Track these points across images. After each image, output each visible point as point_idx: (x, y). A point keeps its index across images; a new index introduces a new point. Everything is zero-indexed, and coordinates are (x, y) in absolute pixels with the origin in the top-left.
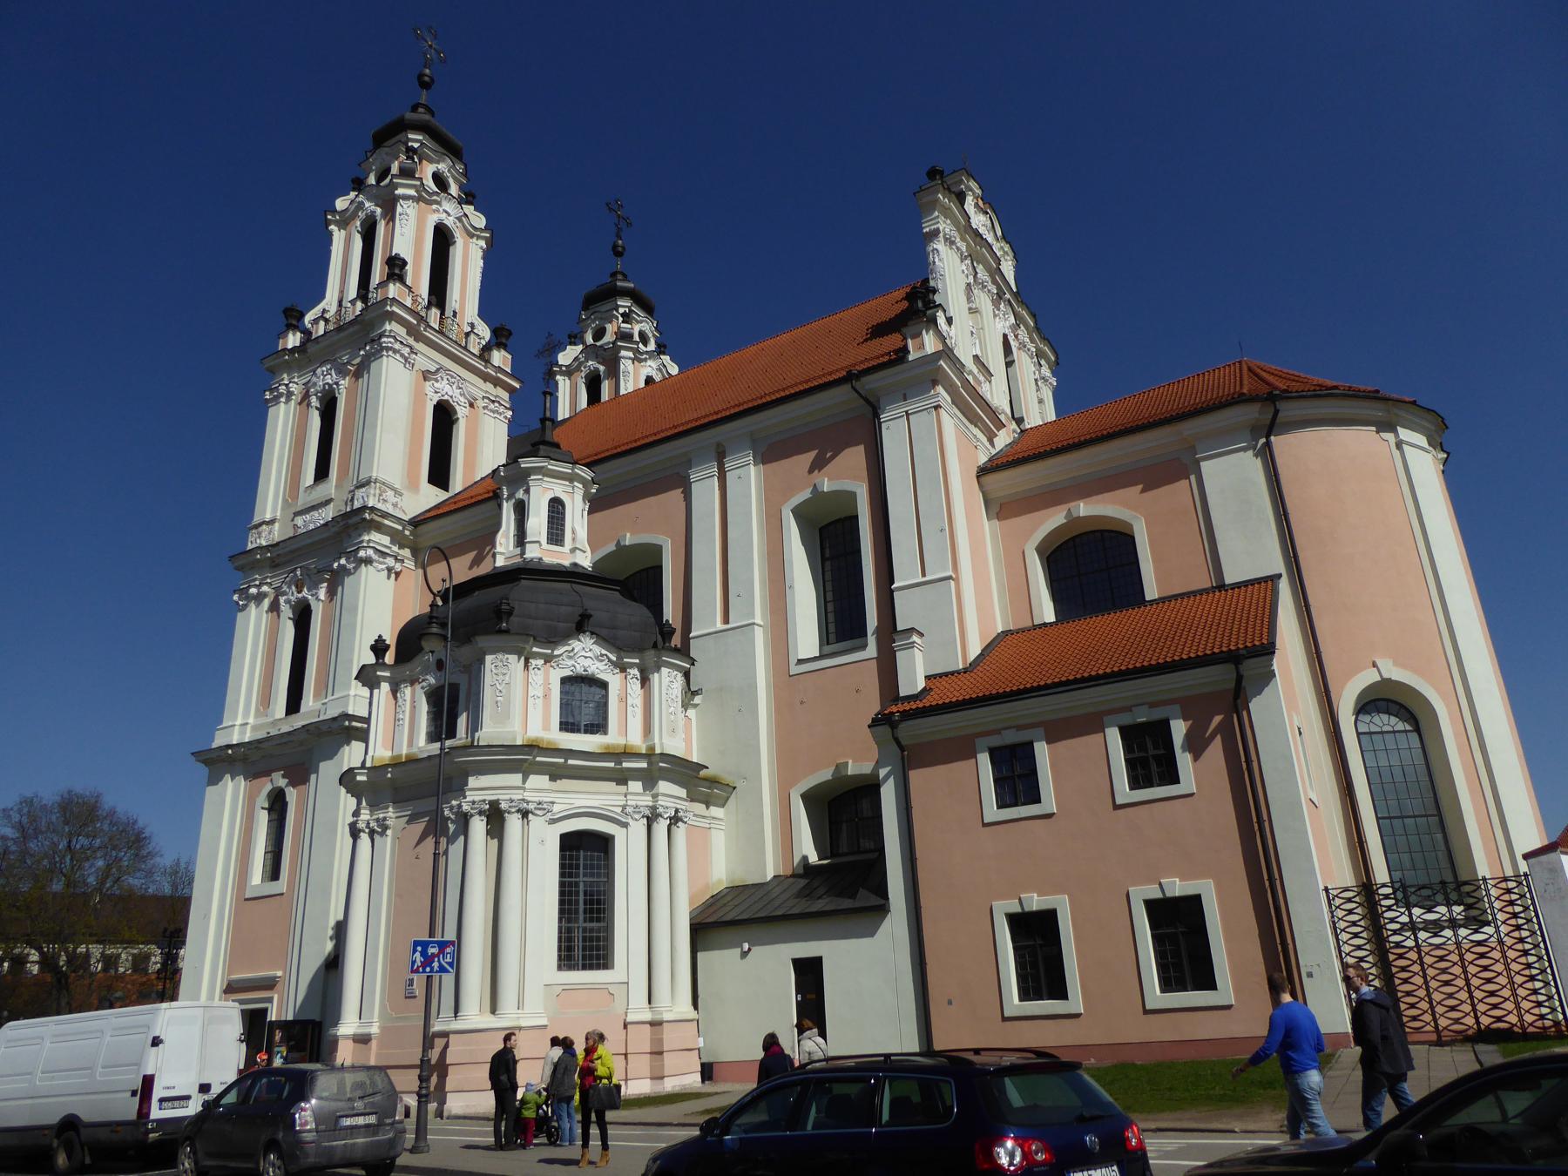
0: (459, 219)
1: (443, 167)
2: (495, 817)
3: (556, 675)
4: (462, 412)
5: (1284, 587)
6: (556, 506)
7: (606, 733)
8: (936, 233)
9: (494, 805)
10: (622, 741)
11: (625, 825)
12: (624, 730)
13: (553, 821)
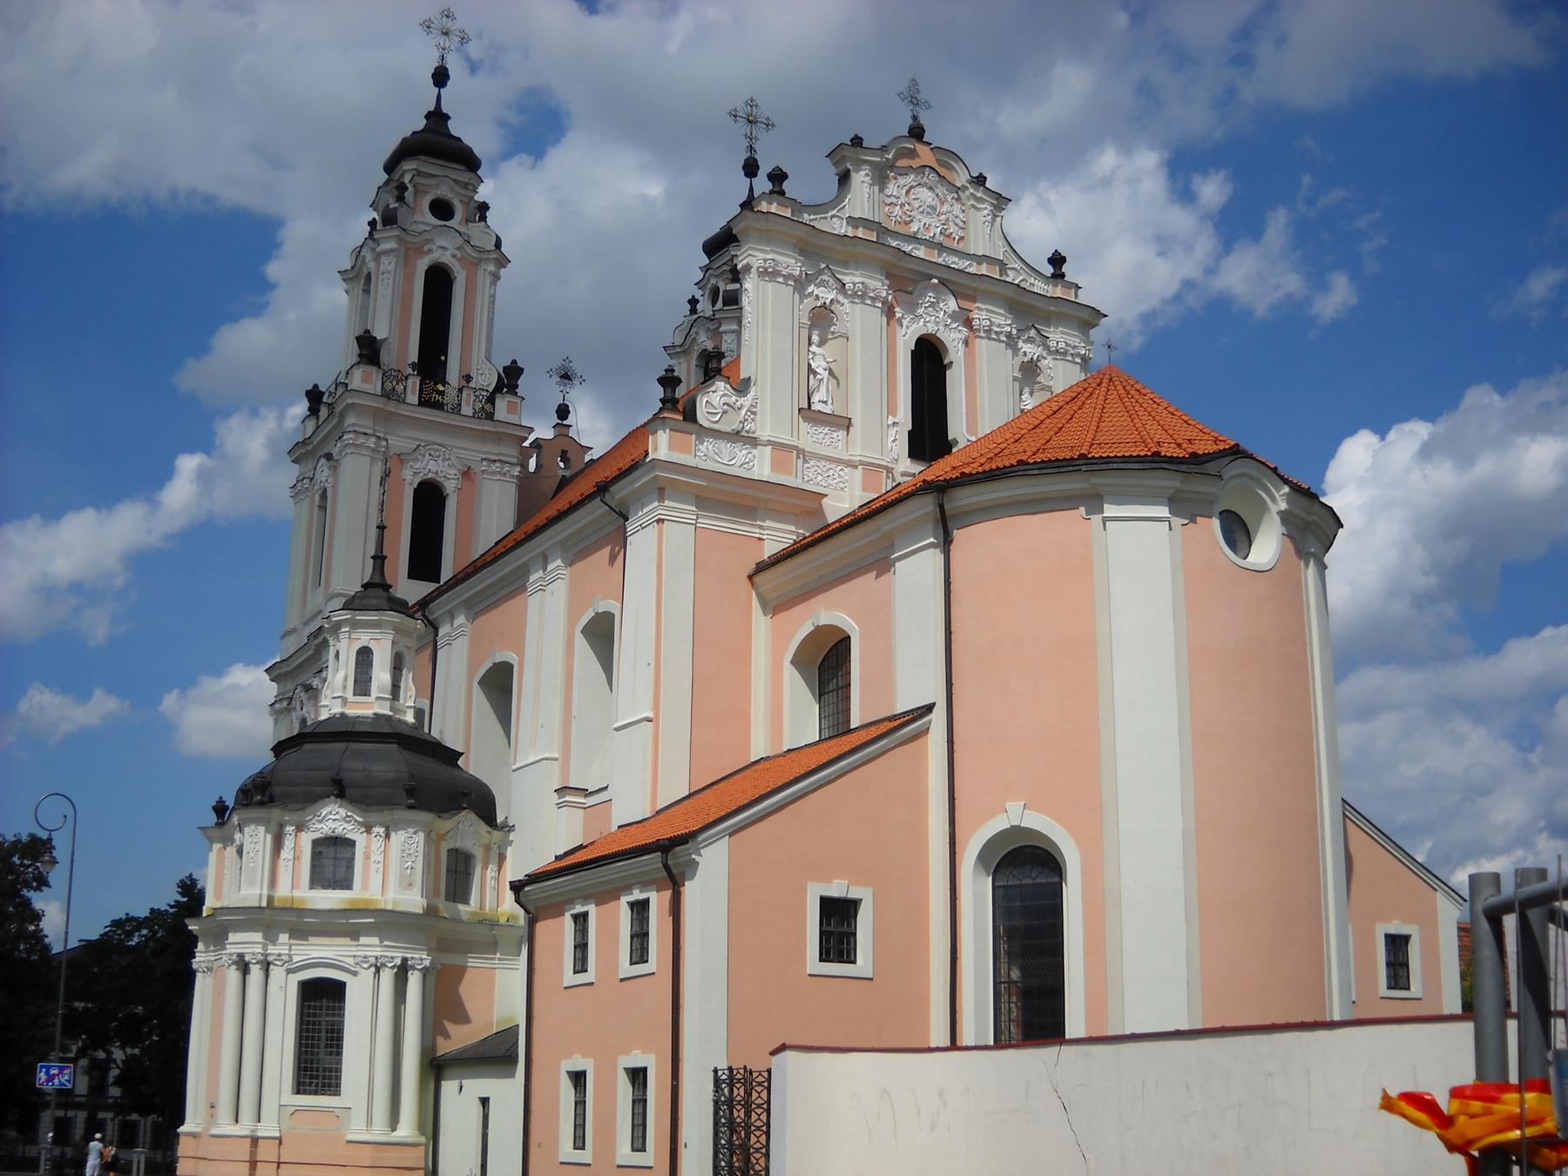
0: (460, 248)
1: (444, 191)
2: (244, 968)
3: (306, 839)
4: (450, 487)
5: (938, 719)
6: (365, 655)
7: (349, 887)
8: (748, 268)
9: (241, 956)
10: (366, 895)
11: (355, 974)
12: (365, 886)
13: (289, 971)
